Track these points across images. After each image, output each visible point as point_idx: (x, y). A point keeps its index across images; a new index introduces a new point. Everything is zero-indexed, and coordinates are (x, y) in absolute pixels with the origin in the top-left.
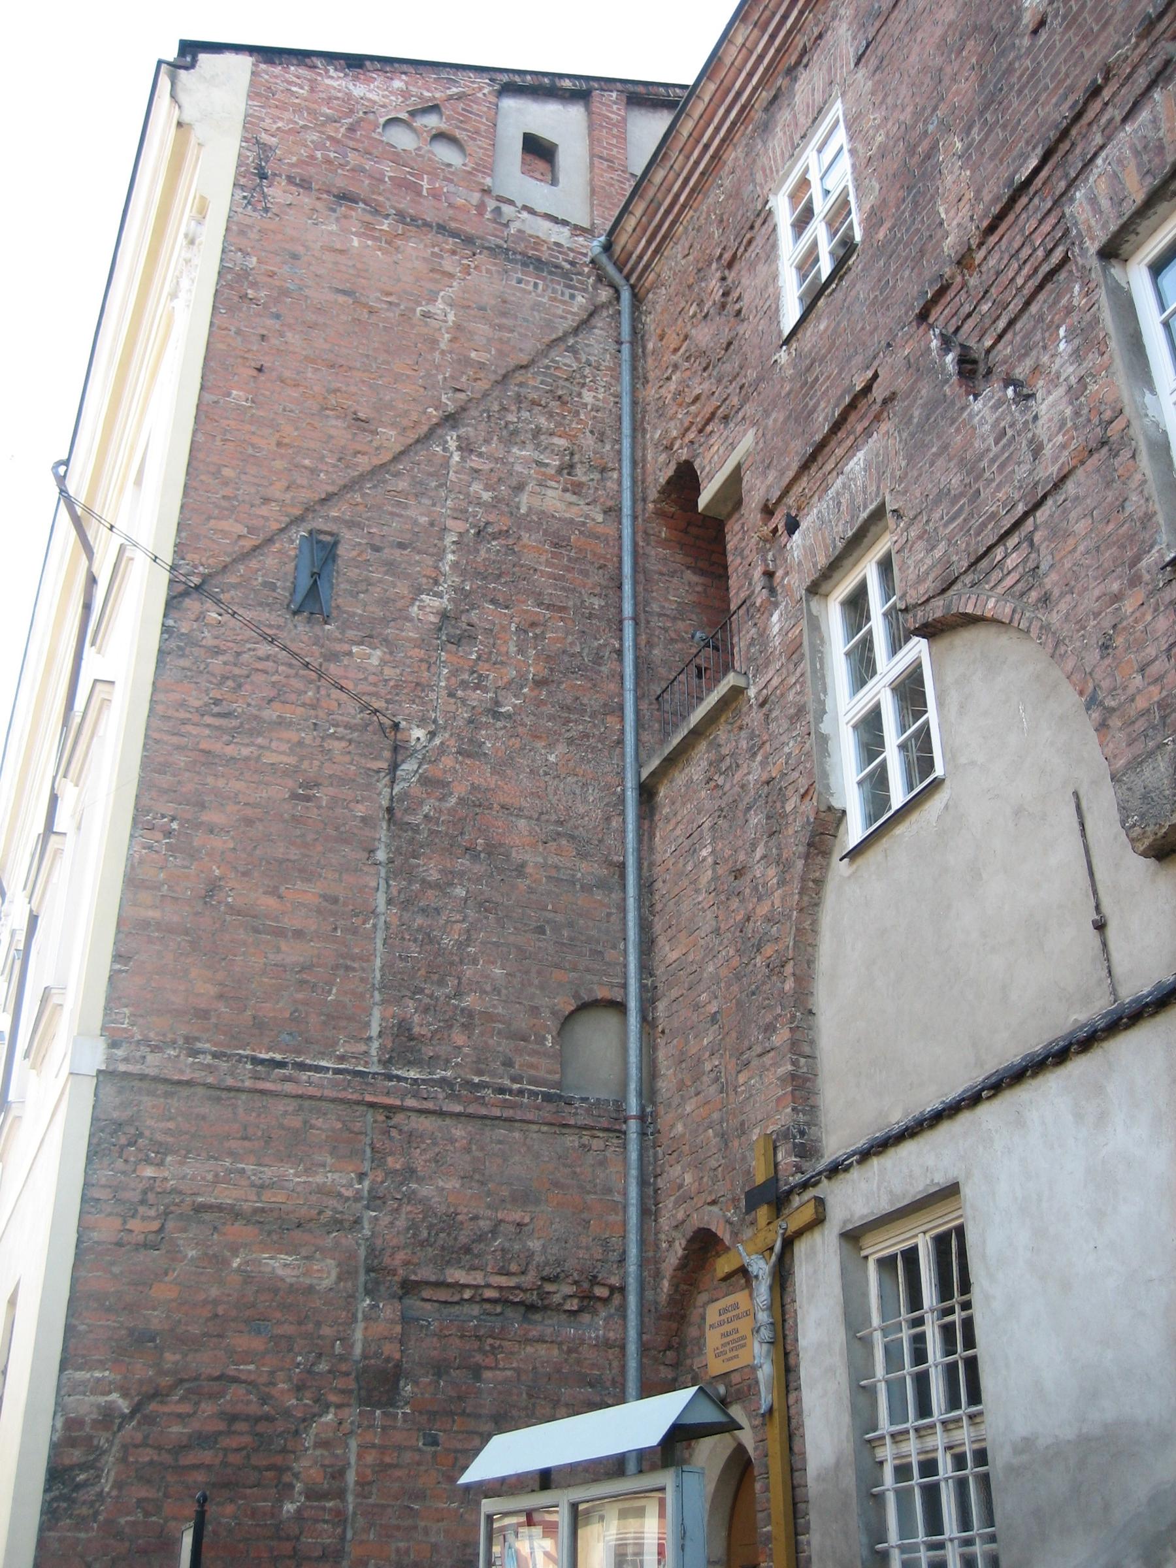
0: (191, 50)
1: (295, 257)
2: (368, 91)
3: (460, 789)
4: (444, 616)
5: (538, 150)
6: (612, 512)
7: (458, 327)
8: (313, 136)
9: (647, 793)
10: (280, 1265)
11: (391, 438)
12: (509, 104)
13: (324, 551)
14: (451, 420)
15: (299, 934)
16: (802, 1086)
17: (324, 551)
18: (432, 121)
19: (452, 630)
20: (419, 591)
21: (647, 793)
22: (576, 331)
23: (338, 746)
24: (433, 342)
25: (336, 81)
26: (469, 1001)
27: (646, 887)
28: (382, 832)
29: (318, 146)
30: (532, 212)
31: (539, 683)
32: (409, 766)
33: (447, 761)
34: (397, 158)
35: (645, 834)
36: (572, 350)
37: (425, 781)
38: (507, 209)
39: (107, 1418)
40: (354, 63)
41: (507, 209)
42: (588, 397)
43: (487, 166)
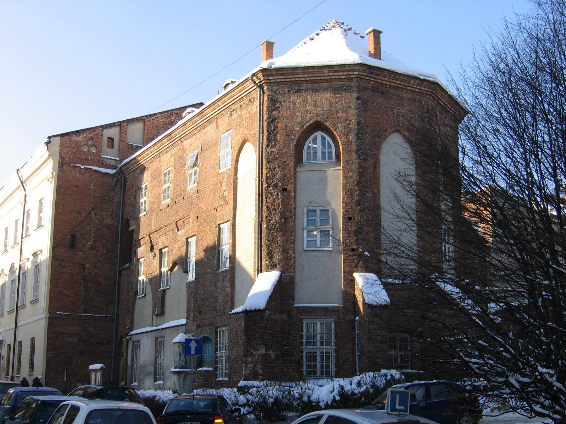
0: (49, 138)
1: (68, 181)
2: (79, 139)
3: (93, 273)
4: (91, 245)
5: (111, 140)
8: (70, 153)
9: (120, 272)
10: (70, 339)
11: (83, 215)
12: (105, 131)
13: (74, 237)
14: (93, 209)
15: (72, 297)
17: (74, 237)
19: (93, 247)
20: (88, 242)
21: (120, 272)
22: (114, 186)
23: (76, 269)
25: (74, 138)
26: (94, 304)
27: (119, 286)
28: (83, 281)
29: (72, 155)
31: (105, 254)
32: (86, 271)
33: (92, 269)
34: (85, 153)
35: (119, 278)
36: (113, 191)
37: (89, 273)
39: (52, 357)
40: (77, 133)
42: (115, 199)
43: (100, 151)
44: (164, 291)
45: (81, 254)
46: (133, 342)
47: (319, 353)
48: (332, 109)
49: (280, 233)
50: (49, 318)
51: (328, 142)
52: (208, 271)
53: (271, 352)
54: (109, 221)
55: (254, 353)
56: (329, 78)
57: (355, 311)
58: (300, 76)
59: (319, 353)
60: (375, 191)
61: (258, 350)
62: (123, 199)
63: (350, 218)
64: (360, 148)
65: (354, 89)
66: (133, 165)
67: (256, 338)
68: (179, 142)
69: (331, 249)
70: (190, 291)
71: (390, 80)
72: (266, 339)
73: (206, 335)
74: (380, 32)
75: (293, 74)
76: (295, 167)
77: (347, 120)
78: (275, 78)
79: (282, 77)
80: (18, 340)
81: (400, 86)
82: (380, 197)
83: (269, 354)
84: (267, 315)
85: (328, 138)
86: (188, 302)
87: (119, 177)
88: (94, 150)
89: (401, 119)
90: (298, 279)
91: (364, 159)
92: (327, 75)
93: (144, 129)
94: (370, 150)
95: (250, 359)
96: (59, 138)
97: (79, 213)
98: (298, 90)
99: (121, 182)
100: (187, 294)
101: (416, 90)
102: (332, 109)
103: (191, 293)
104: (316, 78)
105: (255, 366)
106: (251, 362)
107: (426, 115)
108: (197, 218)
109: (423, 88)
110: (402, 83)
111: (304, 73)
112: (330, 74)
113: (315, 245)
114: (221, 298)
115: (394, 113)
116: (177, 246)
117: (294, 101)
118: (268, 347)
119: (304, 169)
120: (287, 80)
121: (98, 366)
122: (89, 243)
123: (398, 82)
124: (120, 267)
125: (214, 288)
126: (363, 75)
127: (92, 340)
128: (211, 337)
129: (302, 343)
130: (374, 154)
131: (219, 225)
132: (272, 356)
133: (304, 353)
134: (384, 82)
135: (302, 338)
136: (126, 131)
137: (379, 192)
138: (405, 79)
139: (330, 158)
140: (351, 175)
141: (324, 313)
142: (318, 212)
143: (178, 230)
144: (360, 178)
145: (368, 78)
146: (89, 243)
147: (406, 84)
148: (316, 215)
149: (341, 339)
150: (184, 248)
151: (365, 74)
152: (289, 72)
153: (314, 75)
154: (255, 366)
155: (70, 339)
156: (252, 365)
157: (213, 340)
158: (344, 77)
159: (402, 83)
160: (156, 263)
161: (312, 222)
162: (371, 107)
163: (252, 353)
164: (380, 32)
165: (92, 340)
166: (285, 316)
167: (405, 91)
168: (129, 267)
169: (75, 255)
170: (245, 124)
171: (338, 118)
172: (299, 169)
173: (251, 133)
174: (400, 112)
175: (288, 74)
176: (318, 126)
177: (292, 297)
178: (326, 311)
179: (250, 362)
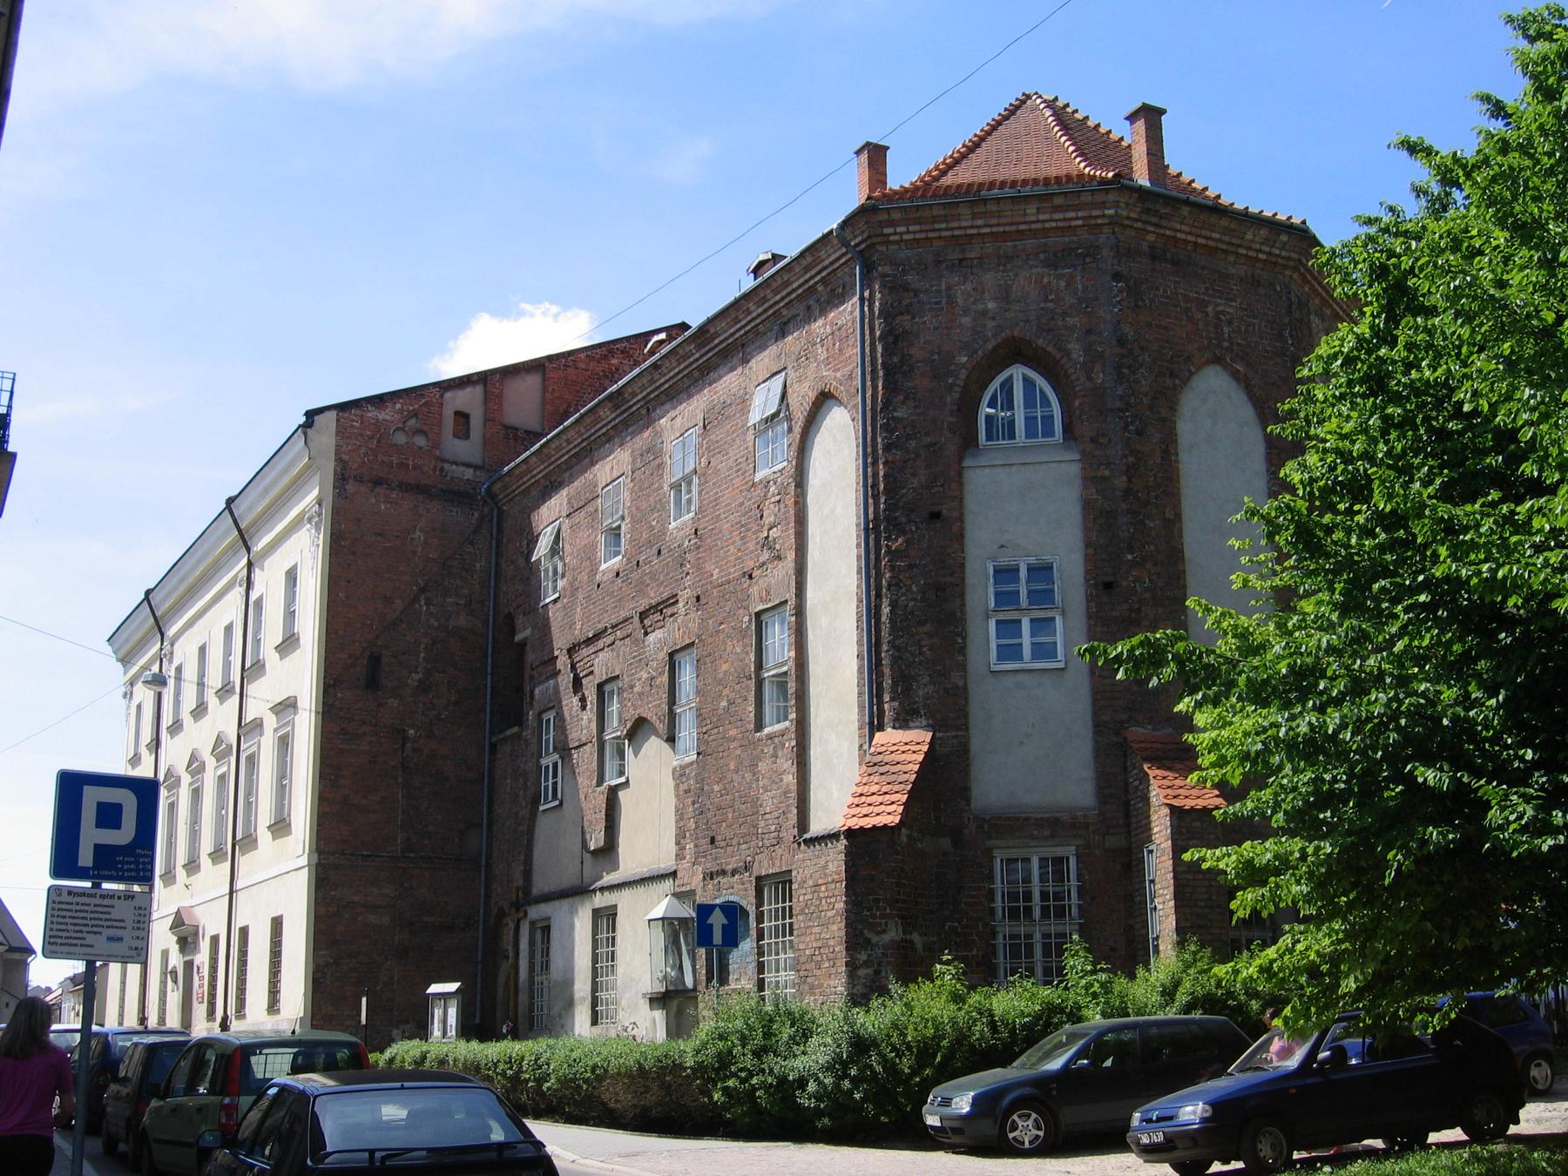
0: (311, 415)
2: (385, 415)
4: (420, 681)
5: (462, 417)
6: (486, 622)
7: (426, 543)
8: (363, 450)
9: (493, 747)
11: (399, 604)
12: (448, 395)
13: (375, 661)
14: (422, 590)
16: (527, 874)
17: (375, 661)
18: (412, 422)
19: (424, 687)
21: (493, 747)
24: (414, 553)
25: (372, 413)
26: (431, 828)
27: (491, 780)
29: (366, 455)
30: (455, 463)
35: (492, 762)
37: (415, 750)
38: (447, 466)
39: (327, 964)
41: (447, 466)
43: (436, 444)
44: (613, 791)
45: (394, 703)
46: (532, 923)
47: (1037, 937)
48: (1051, 305)
49: (928, 628)
50: (318, 865)
51: (1041, 391)
52: (733, 733)
53: (916, 937)
54: (462, 621)
55: (875, 939)
56: (1039, 226)
57: (1129, 825)
58: (964, 224)
59: (1037, 937)
60: (1169, 515)
61: (884, 931)
62: (497, 565)
63: (1108, 586)
64: (1128, 404)
65: (1104, 253)
66: (521, 477)
67: (877, 901)
68: (644, 411)
69: (1061, 665)
70: (683, 787)
72: (904, 901)
73: (732, 898)
74: (1162, 112)
75: (945, 219)
76: (961, 458)
77: (1089, 332)
78: (899, 230)
79: (917, 228)
80: (239, 922)
81: (1220, 245)
82: (1181, 529)
83: (912, 942)
84: (904, 839)
85: (1041, 382)
86: (680, 815)
87: (486, 510)
88: (420, 441)
89: (1226, 330)
90: (975, 745)
91: (1139, 433)
92: (1033, 218)
93: (544, 390)
94: (1151, 408)
95: (863, 957)
96: (333, 414)
97: (388, 600)
98: (961, 260)
99: (491, 521)
100: (677, 796)
102: (1051, 305)
103: (687, 792)
104: (1007, 229)
105: (877, 972)
106: (866, 964)
107: (1287, 320)
108: (698, 598)
111: (974, 216)
112: (1042, 217)
113: (1020, 658)
114: (769, 802)
116: (645, 675)
117: (949, 288)
118: (908, 923)
119: (983, 461)
120: (931, 235)
121: (452, 987)
122: (416, 677)
124: (492, 733)
125: (748, 776)
126: (1128, 218)
127: (426, 919)
128: (744, 903)
129: (992, 911)
130: (1164, 420)
131: (758, 614)
132: (919, 946)
133: (1000, 939)
134: (1179, 235)
135: (993, 900)
136: (500, 396)
137: (1178, 516)
139: (1048, 432)
140: (1107, 473)
141: (1047, 833)
142: (1023, 573)
143: (646, 634)
144: (1129, 481)
146: (416, 677)
148: (1017, 580)
149: (1093, 898)
150: (665, 678)
151: (1132, 215)
152: (935, 213)
153: (1002, 220)
154: (877, 972)
155: (372, 918)
156: (869, 971)
157: (752, 910)
158: (1079, 222)
159: (1227, 239)
160: (590, 721)
161: (1006, 599)
162: (1152, 300)
163: (868, 941)
164: (1162, 112)
165: (426, 919)
166: (946, 843)
167: (1231, 258)
168: (518, 736)
169: (381, 705)
170: (821, 353)
171: (1066, 328)
172: (967, 462)
173: (838, 375)
174: (1222, 312)
175: (935, 220)
176: (1016, 351)
177: (964, 791)
178: (1052, 825)
179: (865, 962)
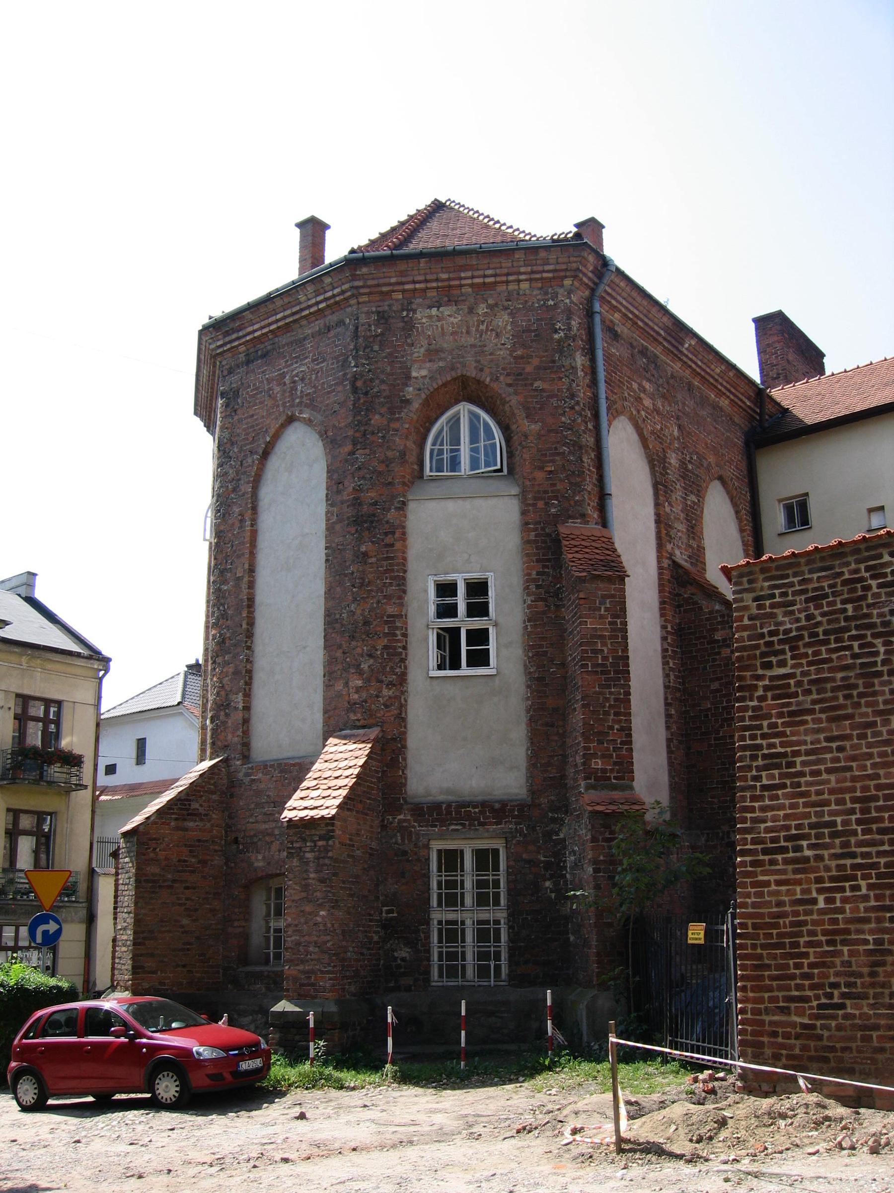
71: (263, 323)
81: (287, 321)
101: (321, 306)
109: (330, 294)
110: (288, 312)
115: (285, 384)
123: (279, 316)
134: (256, 334)
138: (286, 300)
145: (229, 346)
147: (294, 310)
151: (219, 343)
159: (288, 312)
167: (304, 322)
